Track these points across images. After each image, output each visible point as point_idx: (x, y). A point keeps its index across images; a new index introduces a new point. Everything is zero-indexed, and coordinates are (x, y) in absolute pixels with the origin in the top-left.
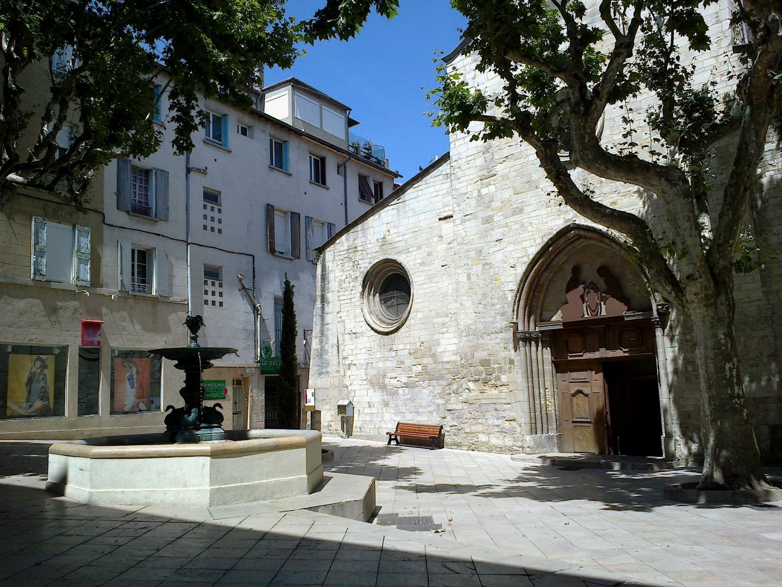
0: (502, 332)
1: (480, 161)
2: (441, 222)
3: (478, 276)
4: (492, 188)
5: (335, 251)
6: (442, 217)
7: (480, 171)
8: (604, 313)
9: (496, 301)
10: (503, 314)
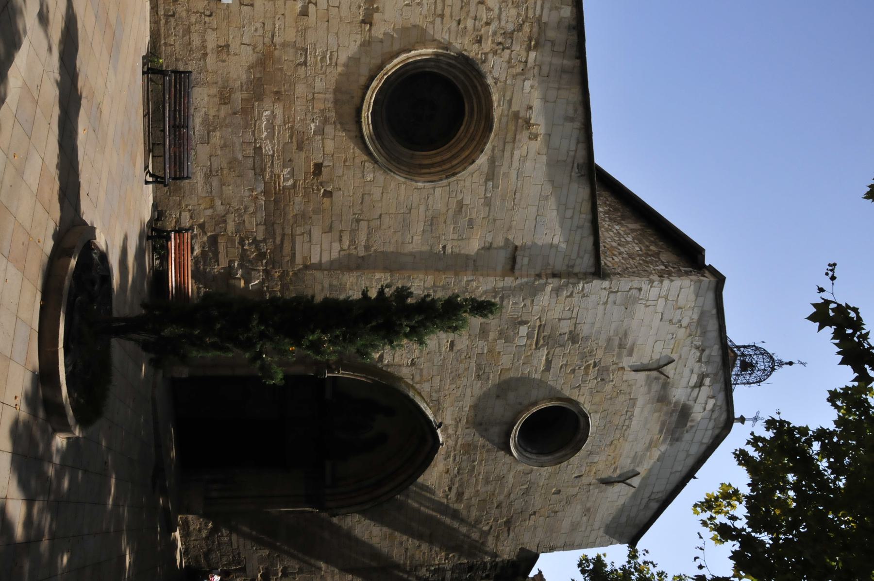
6: (518, 253)
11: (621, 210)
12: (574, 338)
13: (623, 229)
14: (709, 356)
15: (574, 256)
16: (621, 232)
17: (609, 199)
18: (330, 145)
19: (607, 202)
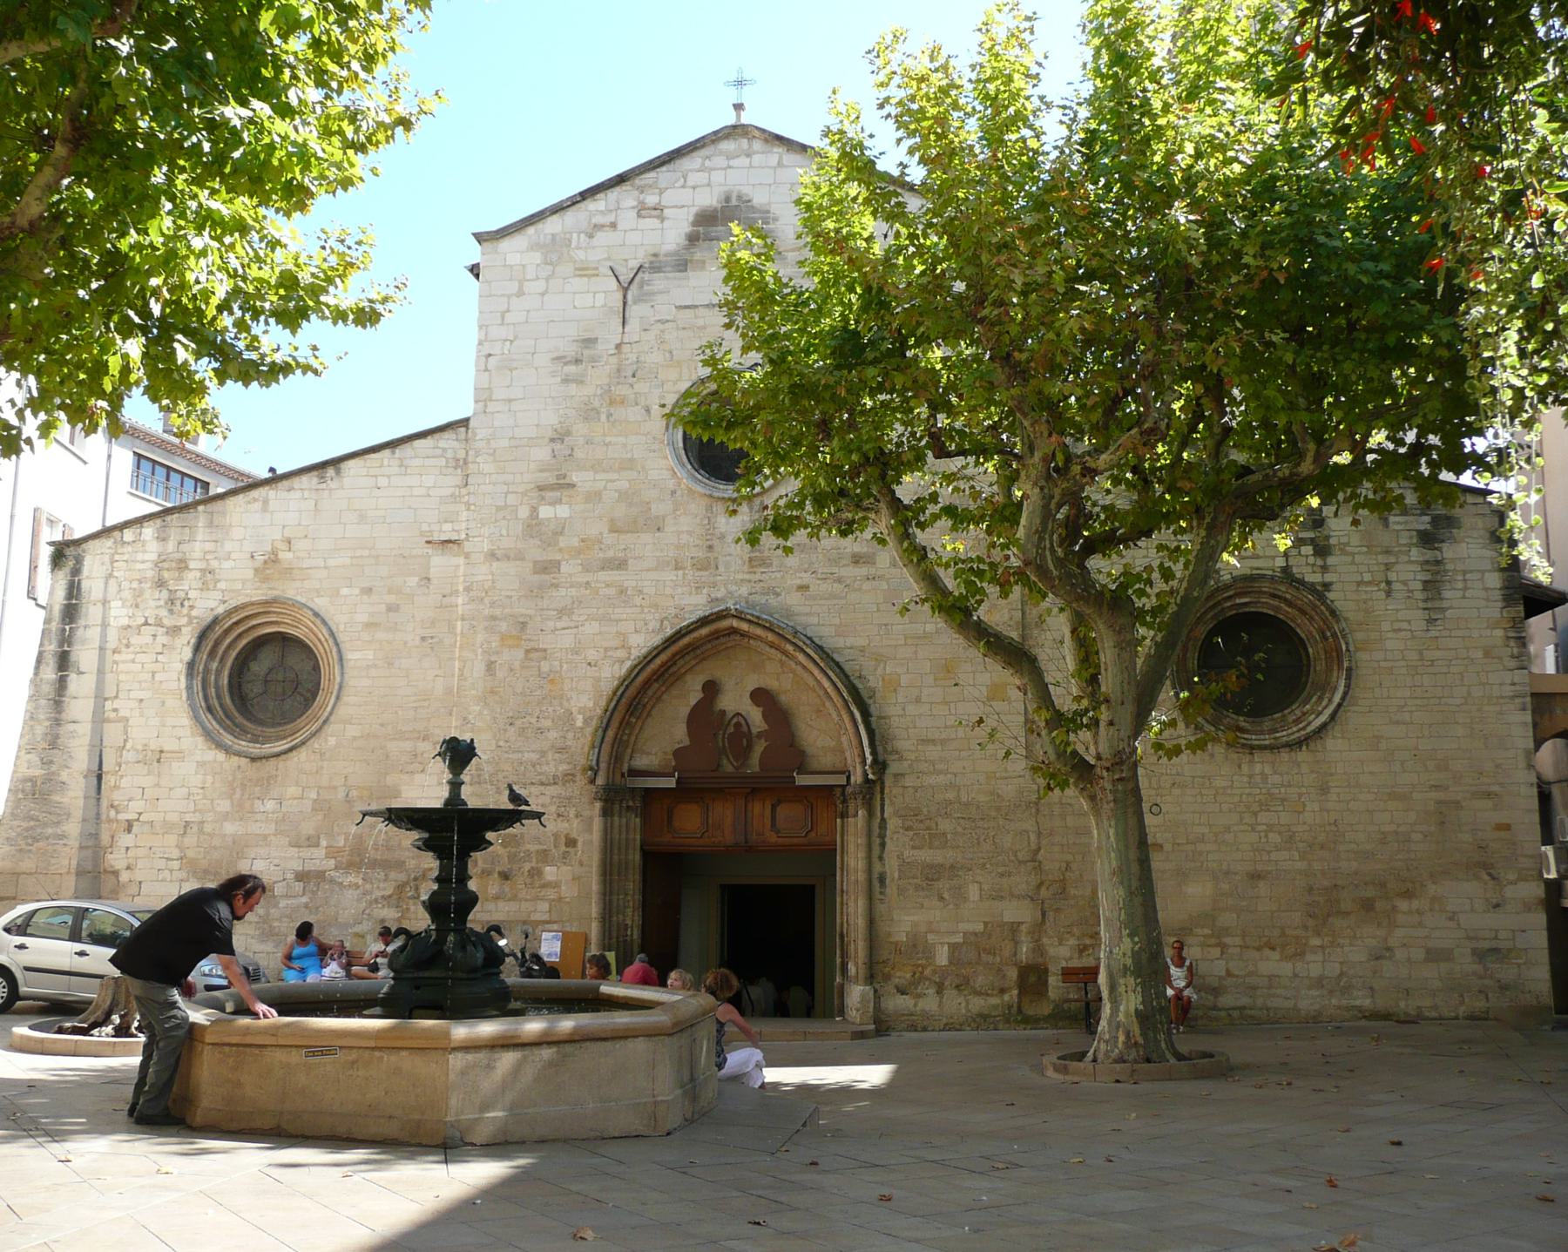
1: (542, 454)
2: (429, 550)
4: (563, 511)
5: (117, 557)
6: (436, 537)
7: (541, 471)
9: (547, 723)
10: (561, 750)
12: (560, 436)
15: (443, 462)
18: (292, 791)
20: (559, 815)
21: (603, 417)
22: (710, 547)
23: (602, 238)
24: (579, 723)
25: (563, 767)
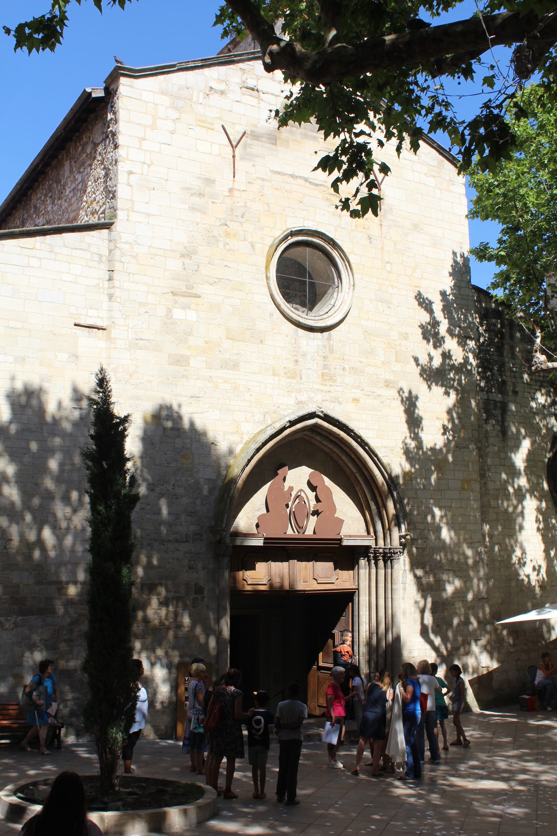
0: (187, 541)
3: (153, 444)
4: (191, 315)
6: (82, 323)
8: (309, 532)
9: (181, 491)
11: (51, 182)
12: (187, 254)
13: (70, 183)
14: (219, 81)
16: (72, 188)
17: (39, 196)
19: (43, 198)
20: (190, 568)
21: (221, 245)
22: (297, 361)
23: (215, 97)
24: (205, 492)
25: (193, 528)
